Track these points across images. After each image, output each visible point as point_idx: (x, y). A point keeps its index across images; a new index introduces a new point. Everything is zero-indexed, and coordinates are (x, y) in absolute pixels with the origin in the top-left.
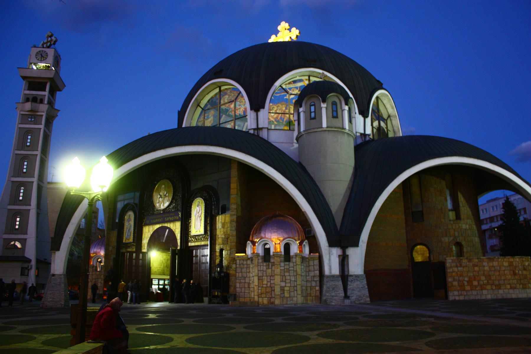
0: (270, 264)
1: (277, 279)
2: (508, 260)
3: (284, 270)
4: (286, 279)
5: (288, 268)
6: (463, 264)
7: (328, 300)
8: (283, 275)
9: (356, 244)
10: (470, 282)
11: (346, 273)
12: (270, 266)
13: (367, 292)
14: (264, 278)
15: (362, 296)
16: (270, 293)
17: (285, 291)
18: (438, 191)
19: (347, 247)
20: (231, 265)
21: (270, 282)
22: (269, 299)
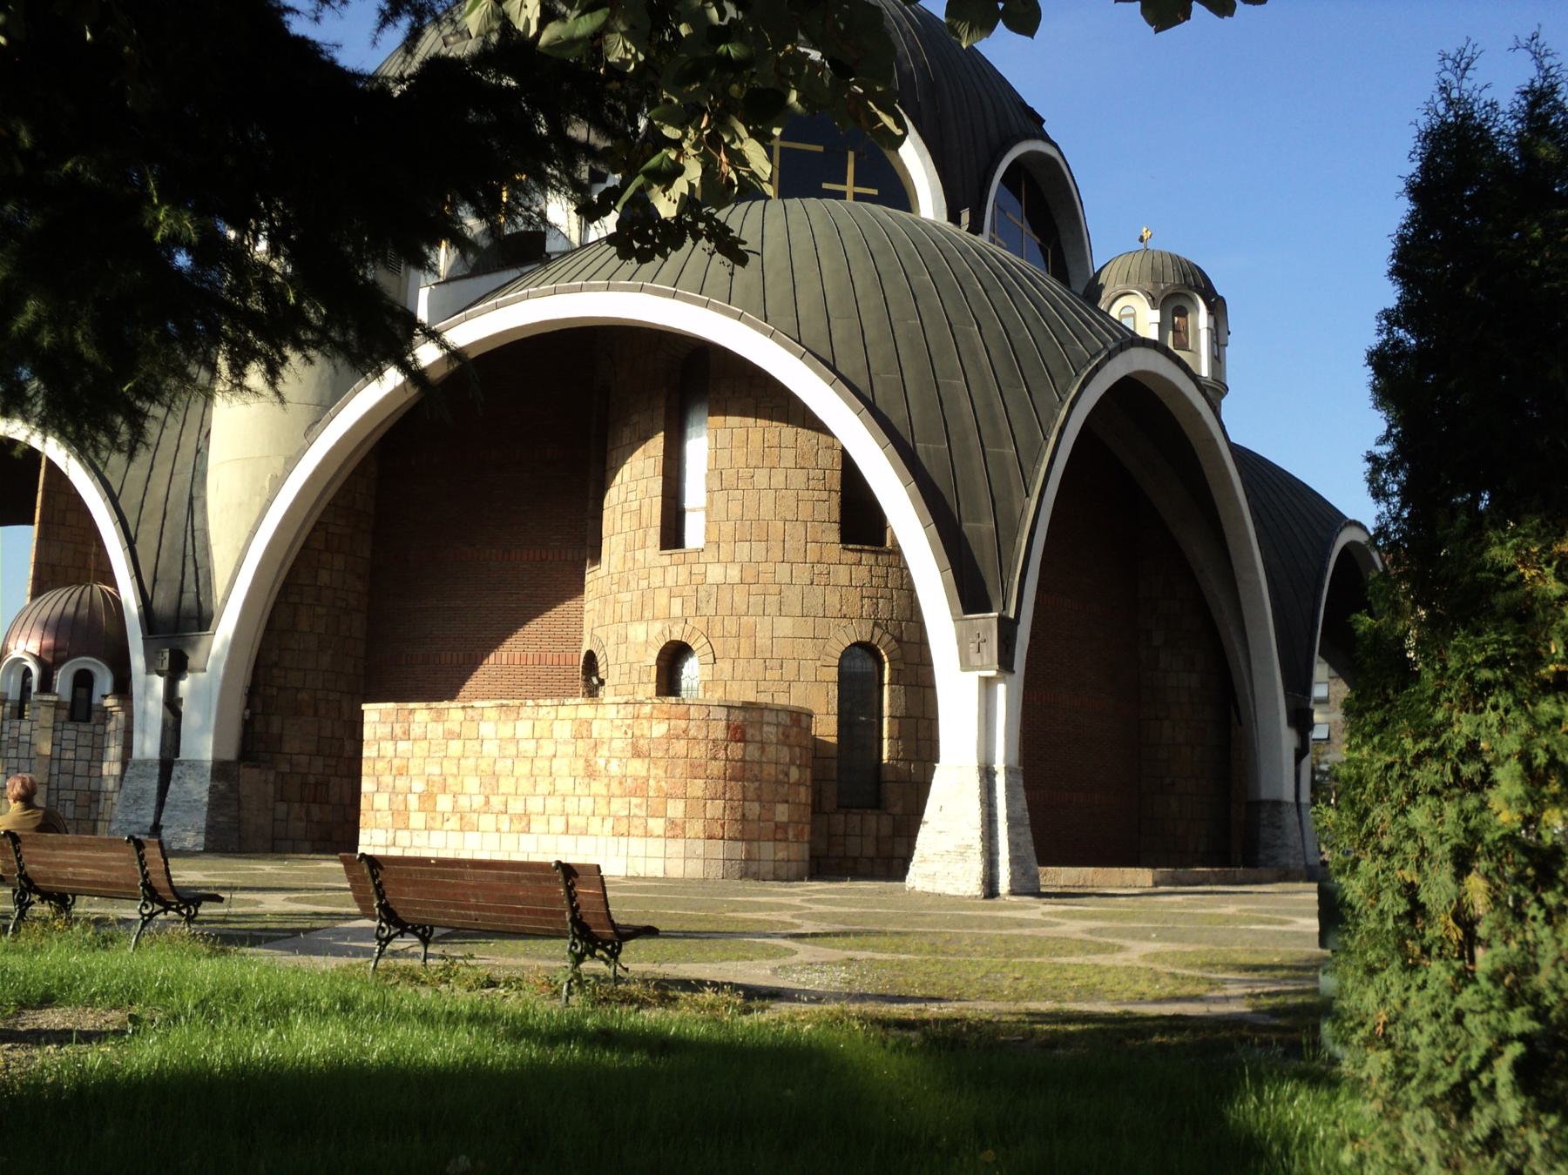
2: (573, 716)
6: (416, 730)
10: (428, 798)
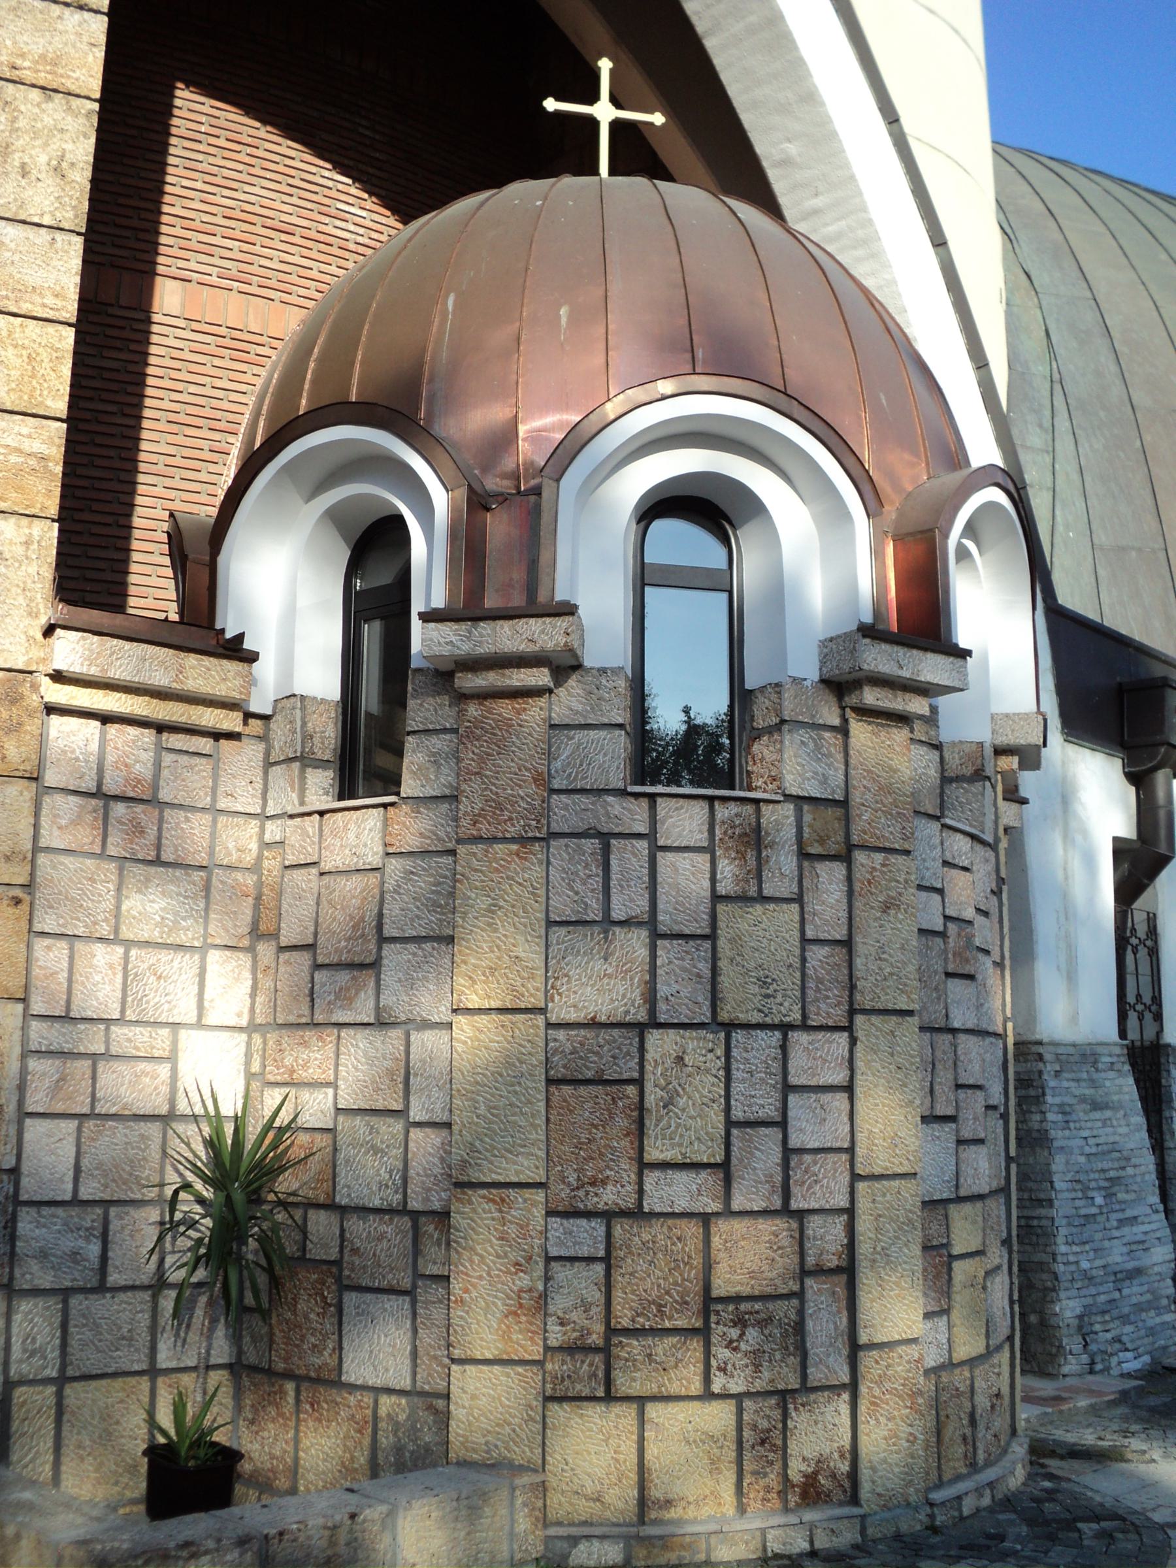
12: (784, 861)
14: (680, 1059)
16: (784, 1310)
21: (782, 1124)
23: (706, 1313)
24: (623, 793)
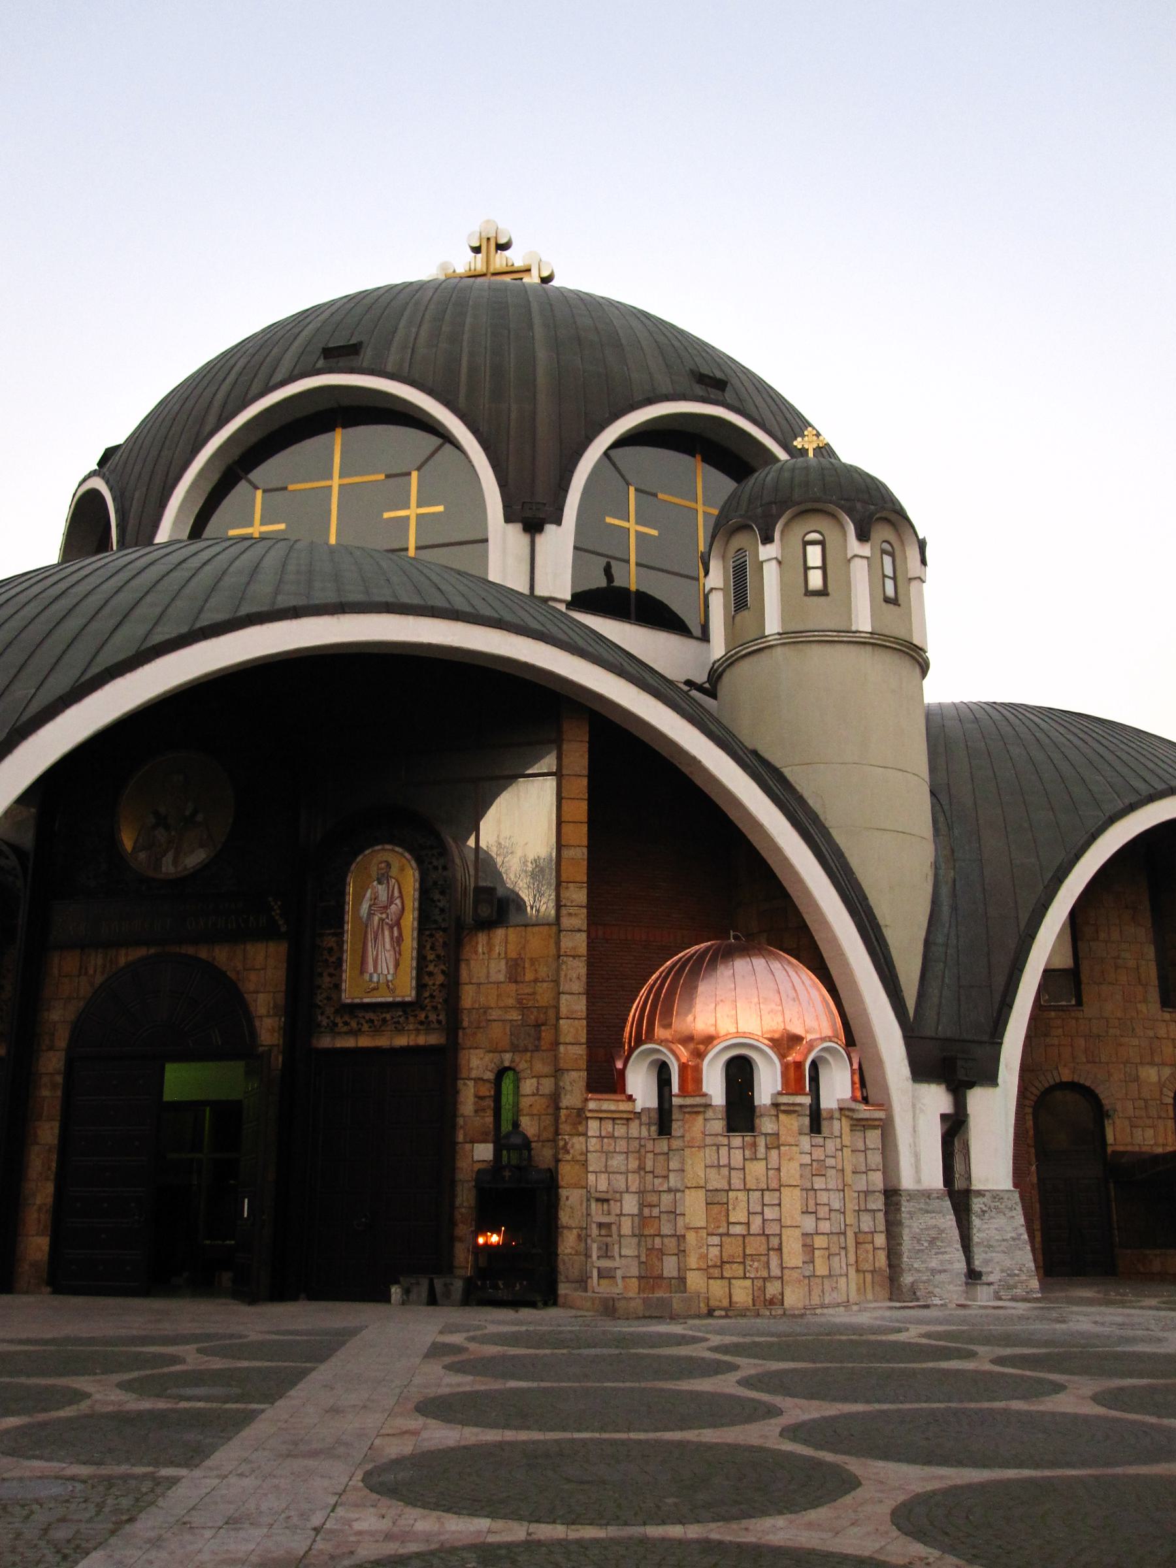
0: (761, 1142)
1: (792, 1200)
3: (811, 1165)
4: (817, 1204)
5: (823, 1158)
7: (921, 1286)
8: (809, 1186)
9: (990, 1078)
11: (959, 1184)
13: (1030, 1256)
14: (737, 1198)
15: (1017, 1272)
16: (764, 1259)
17: (817, 1252)
18: (1127, 907)
19: (971, 1085)
20: (566, 1137)
21: (762, 1213)
22: (759, 1283)
23: (744, 1258)
24: (722, 1135)
